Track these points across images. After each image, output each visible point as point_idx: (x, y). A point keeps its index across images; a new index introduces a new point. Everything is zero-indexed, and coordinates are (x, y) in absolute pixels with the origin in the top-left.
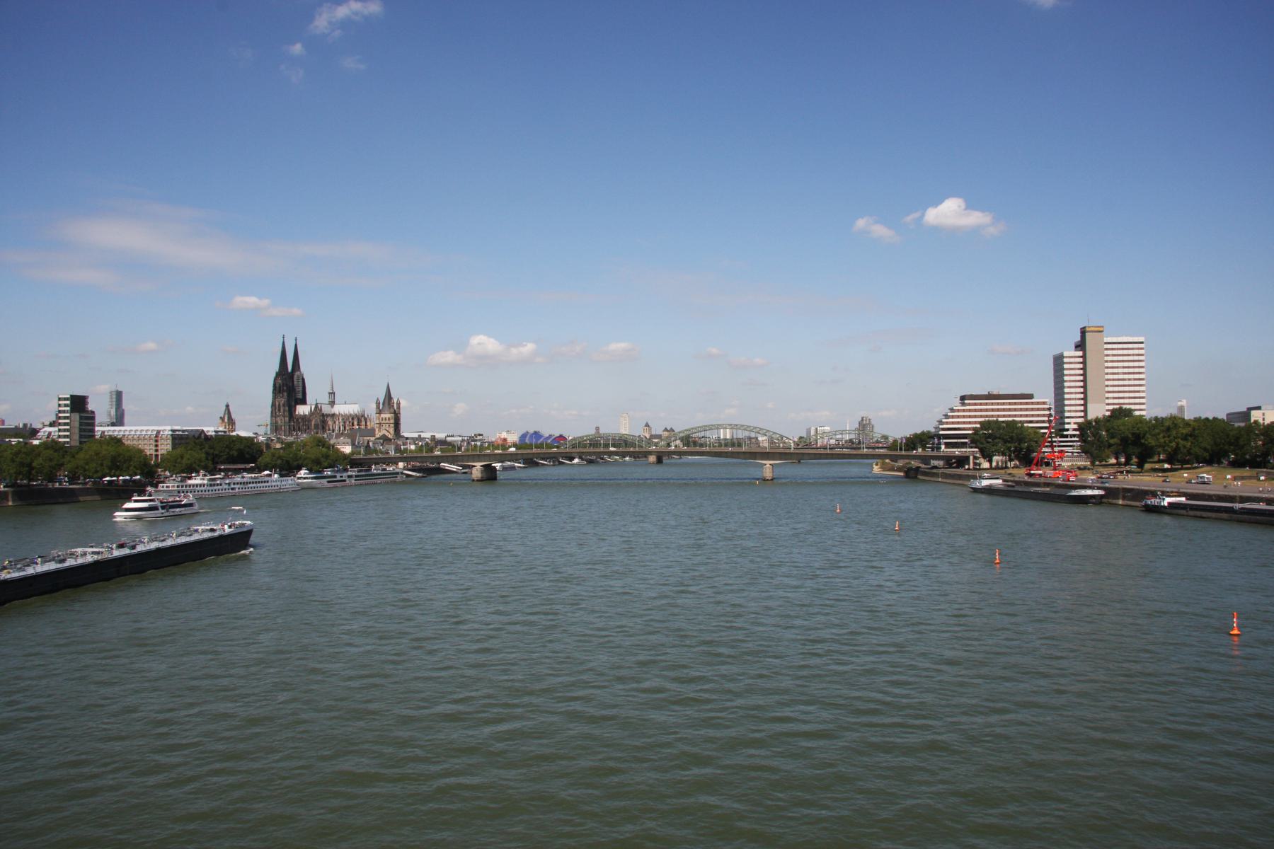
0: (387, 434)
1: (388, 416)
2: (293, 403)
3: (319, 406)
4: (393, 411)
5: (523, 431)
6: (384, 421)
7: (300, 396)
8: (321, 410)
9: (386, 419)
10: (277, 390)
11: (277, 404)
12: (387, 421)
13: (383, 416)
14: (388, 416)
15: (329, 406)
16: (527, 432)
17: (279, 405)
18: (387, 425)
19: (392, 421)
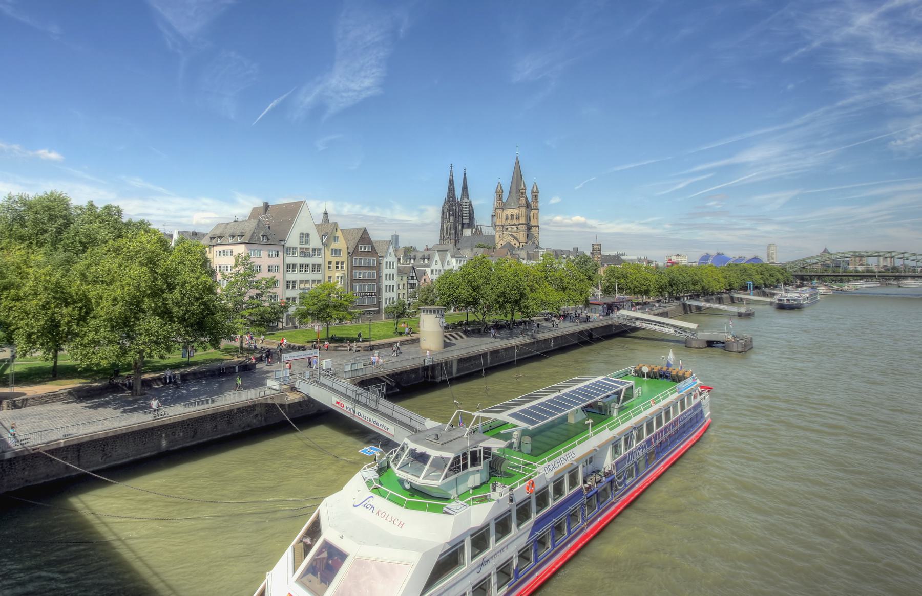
0: (513, 242)
1: (514, 212)
2: (459, 227)
3: (479, 227)
4: (523, 202)
5: (703, 252)
6: (509, 222)
7: (468, 221)
8: (481, 231)
9: (512, 219)
10: (445, 215)
11: (445, 227)
12: (515, 221)
13: (509, 212)
14: (514, 212)
15: (492, 228)
16: (708, 255)
17: (447, 228)
18: (515, 228)
19: (523, 220)
